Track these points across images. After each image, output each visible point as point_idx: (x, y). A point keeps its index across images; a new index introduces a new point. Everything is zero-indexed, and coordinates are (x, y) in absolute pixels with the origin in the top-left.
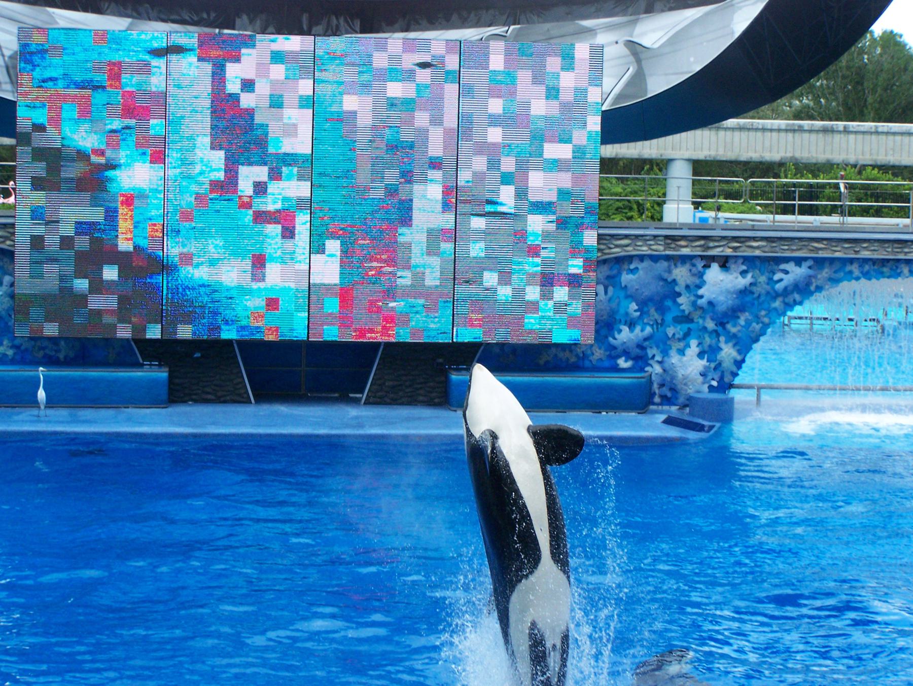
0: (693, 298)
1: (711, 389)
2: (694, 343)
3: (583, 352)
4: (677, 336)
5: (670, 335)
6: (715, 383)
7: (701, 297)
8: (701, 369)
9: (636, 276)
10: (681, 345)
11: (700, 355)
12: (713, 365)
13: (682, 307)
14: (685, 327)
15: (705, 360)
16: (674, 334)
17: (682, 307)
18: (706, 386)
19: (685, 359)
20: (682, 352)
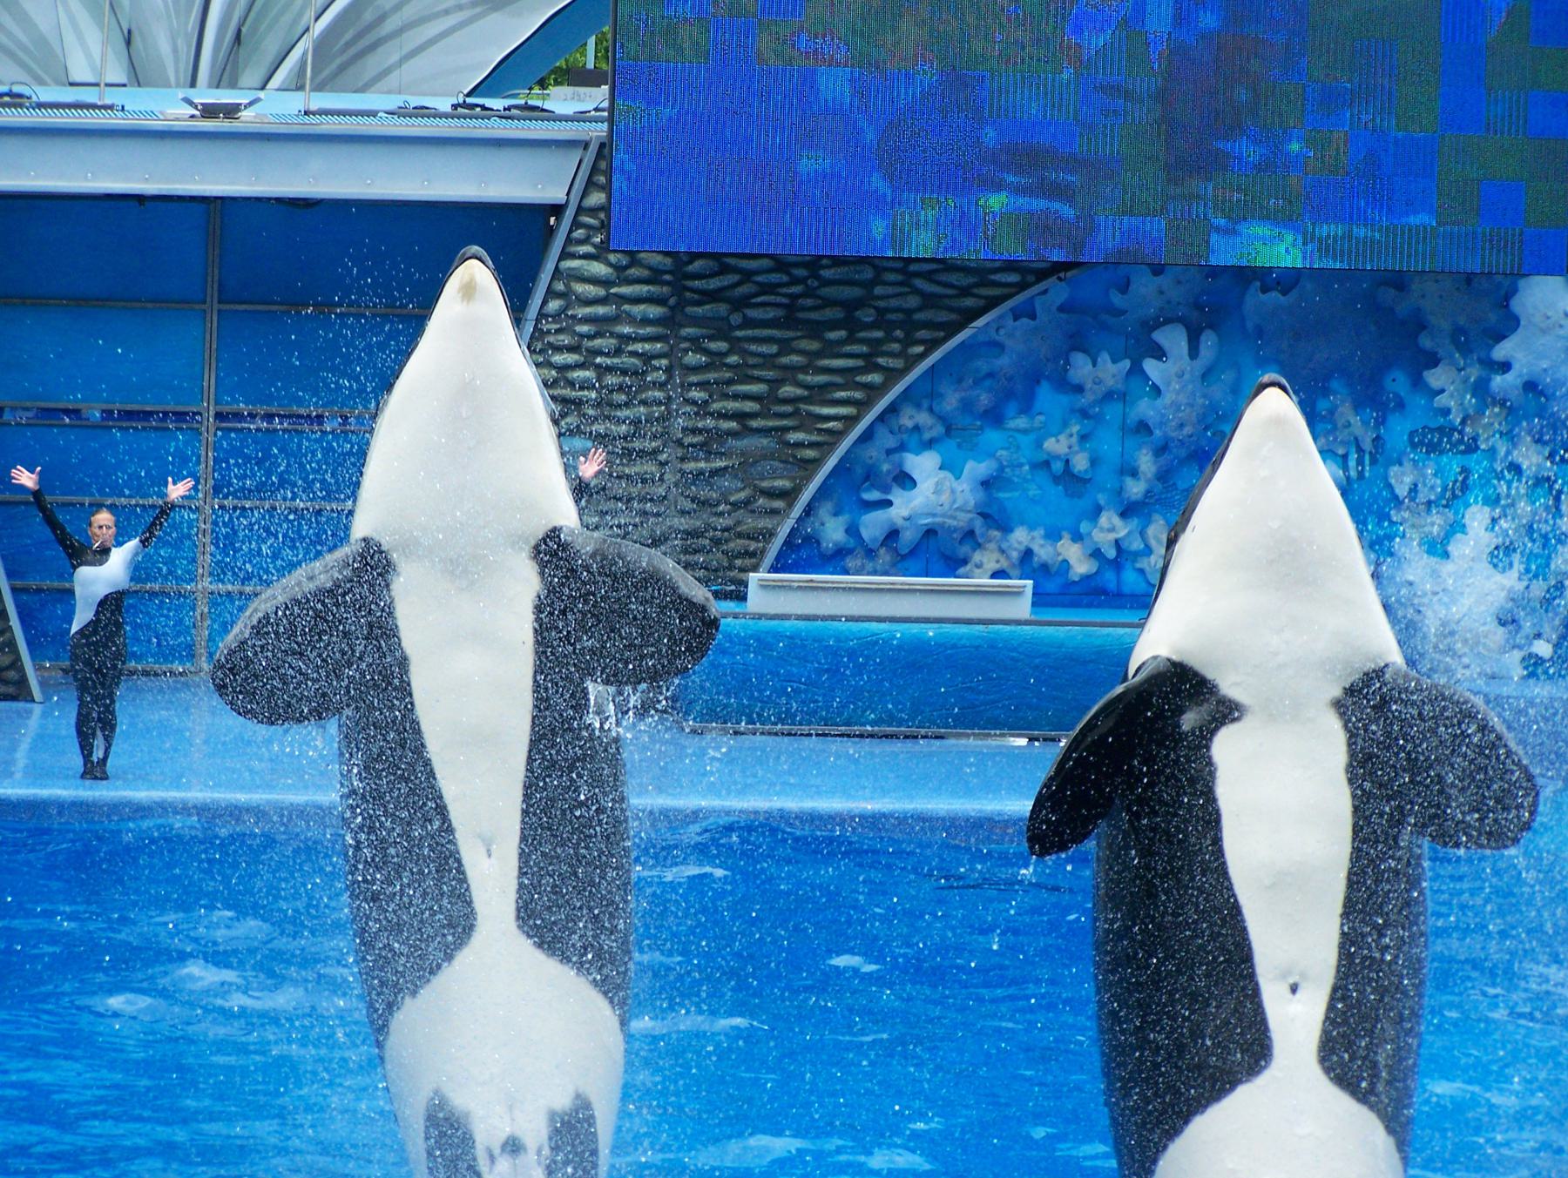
0: (1474, 373)
1: (1534, 665)
2: (1477, 517)
3: (1117, 542)
4: (1422, 497)
5: (1402, 491)
6: (1543, 649)
7: (1505, 367)
8: (1498, 599)
9: (1294, 294)
10: (1435, 523)
11: (1501, 554)
12: (1539, 589)
13: (1442, 401)
14: (1452, 464)
15: (1514, 573)
16: (1414, 489)
17: (1442, 401)
18: (1517, 655)
19: (1448, 567)
20: (1438, 548)
